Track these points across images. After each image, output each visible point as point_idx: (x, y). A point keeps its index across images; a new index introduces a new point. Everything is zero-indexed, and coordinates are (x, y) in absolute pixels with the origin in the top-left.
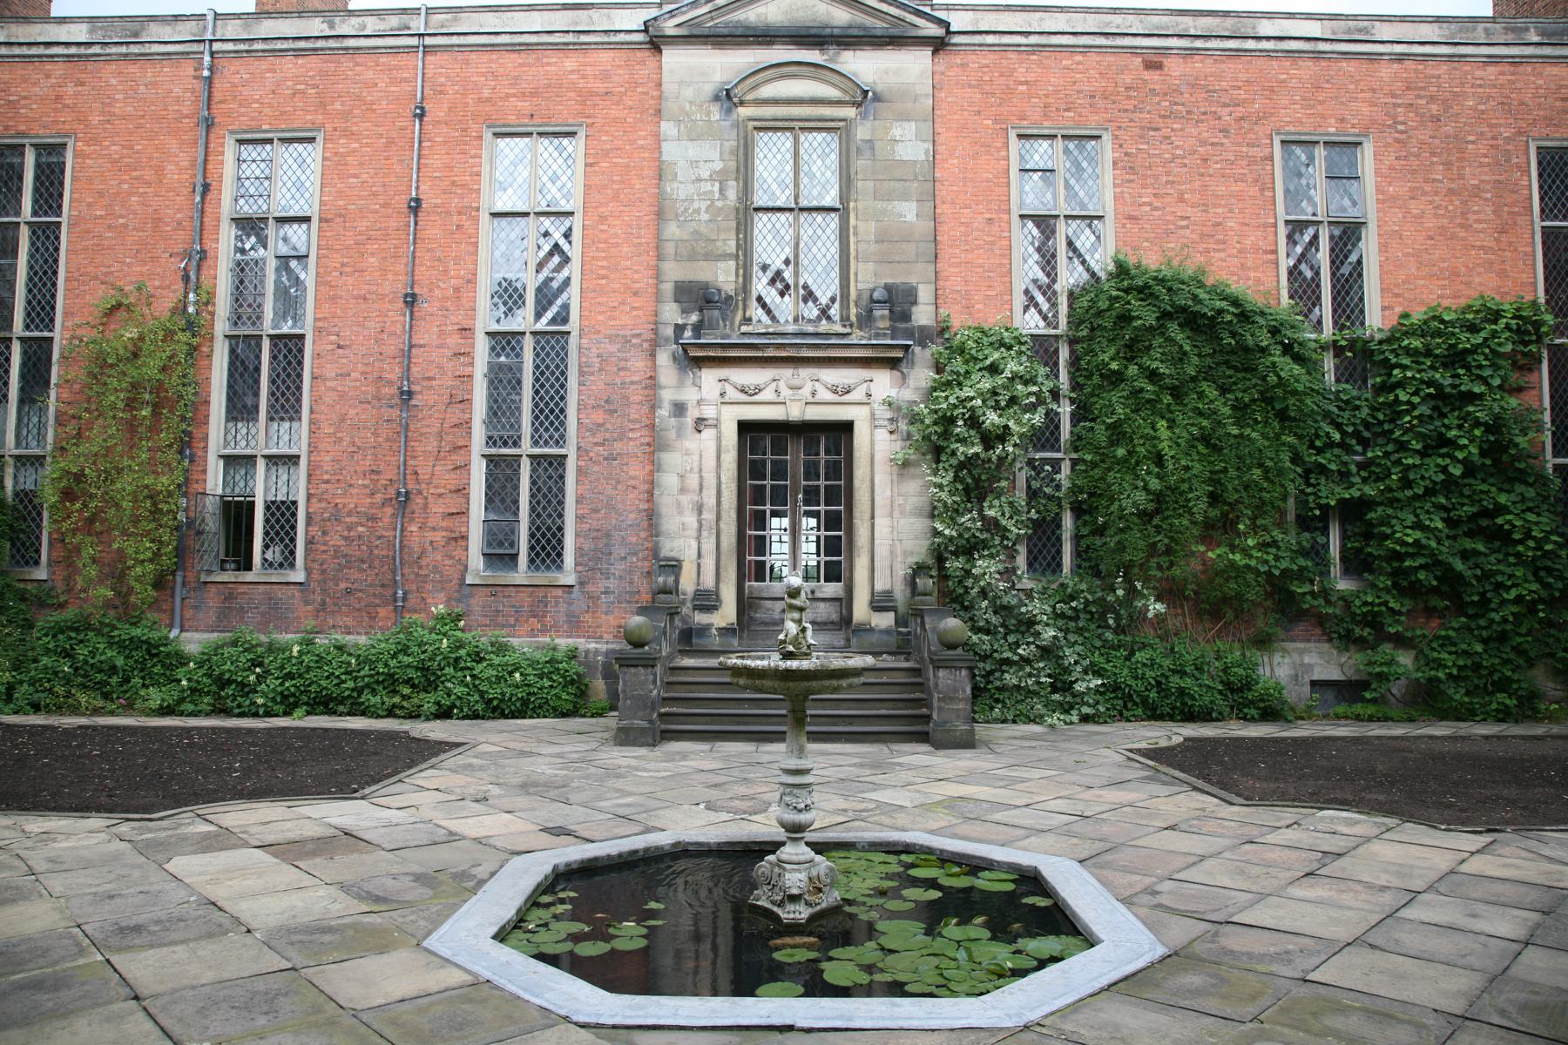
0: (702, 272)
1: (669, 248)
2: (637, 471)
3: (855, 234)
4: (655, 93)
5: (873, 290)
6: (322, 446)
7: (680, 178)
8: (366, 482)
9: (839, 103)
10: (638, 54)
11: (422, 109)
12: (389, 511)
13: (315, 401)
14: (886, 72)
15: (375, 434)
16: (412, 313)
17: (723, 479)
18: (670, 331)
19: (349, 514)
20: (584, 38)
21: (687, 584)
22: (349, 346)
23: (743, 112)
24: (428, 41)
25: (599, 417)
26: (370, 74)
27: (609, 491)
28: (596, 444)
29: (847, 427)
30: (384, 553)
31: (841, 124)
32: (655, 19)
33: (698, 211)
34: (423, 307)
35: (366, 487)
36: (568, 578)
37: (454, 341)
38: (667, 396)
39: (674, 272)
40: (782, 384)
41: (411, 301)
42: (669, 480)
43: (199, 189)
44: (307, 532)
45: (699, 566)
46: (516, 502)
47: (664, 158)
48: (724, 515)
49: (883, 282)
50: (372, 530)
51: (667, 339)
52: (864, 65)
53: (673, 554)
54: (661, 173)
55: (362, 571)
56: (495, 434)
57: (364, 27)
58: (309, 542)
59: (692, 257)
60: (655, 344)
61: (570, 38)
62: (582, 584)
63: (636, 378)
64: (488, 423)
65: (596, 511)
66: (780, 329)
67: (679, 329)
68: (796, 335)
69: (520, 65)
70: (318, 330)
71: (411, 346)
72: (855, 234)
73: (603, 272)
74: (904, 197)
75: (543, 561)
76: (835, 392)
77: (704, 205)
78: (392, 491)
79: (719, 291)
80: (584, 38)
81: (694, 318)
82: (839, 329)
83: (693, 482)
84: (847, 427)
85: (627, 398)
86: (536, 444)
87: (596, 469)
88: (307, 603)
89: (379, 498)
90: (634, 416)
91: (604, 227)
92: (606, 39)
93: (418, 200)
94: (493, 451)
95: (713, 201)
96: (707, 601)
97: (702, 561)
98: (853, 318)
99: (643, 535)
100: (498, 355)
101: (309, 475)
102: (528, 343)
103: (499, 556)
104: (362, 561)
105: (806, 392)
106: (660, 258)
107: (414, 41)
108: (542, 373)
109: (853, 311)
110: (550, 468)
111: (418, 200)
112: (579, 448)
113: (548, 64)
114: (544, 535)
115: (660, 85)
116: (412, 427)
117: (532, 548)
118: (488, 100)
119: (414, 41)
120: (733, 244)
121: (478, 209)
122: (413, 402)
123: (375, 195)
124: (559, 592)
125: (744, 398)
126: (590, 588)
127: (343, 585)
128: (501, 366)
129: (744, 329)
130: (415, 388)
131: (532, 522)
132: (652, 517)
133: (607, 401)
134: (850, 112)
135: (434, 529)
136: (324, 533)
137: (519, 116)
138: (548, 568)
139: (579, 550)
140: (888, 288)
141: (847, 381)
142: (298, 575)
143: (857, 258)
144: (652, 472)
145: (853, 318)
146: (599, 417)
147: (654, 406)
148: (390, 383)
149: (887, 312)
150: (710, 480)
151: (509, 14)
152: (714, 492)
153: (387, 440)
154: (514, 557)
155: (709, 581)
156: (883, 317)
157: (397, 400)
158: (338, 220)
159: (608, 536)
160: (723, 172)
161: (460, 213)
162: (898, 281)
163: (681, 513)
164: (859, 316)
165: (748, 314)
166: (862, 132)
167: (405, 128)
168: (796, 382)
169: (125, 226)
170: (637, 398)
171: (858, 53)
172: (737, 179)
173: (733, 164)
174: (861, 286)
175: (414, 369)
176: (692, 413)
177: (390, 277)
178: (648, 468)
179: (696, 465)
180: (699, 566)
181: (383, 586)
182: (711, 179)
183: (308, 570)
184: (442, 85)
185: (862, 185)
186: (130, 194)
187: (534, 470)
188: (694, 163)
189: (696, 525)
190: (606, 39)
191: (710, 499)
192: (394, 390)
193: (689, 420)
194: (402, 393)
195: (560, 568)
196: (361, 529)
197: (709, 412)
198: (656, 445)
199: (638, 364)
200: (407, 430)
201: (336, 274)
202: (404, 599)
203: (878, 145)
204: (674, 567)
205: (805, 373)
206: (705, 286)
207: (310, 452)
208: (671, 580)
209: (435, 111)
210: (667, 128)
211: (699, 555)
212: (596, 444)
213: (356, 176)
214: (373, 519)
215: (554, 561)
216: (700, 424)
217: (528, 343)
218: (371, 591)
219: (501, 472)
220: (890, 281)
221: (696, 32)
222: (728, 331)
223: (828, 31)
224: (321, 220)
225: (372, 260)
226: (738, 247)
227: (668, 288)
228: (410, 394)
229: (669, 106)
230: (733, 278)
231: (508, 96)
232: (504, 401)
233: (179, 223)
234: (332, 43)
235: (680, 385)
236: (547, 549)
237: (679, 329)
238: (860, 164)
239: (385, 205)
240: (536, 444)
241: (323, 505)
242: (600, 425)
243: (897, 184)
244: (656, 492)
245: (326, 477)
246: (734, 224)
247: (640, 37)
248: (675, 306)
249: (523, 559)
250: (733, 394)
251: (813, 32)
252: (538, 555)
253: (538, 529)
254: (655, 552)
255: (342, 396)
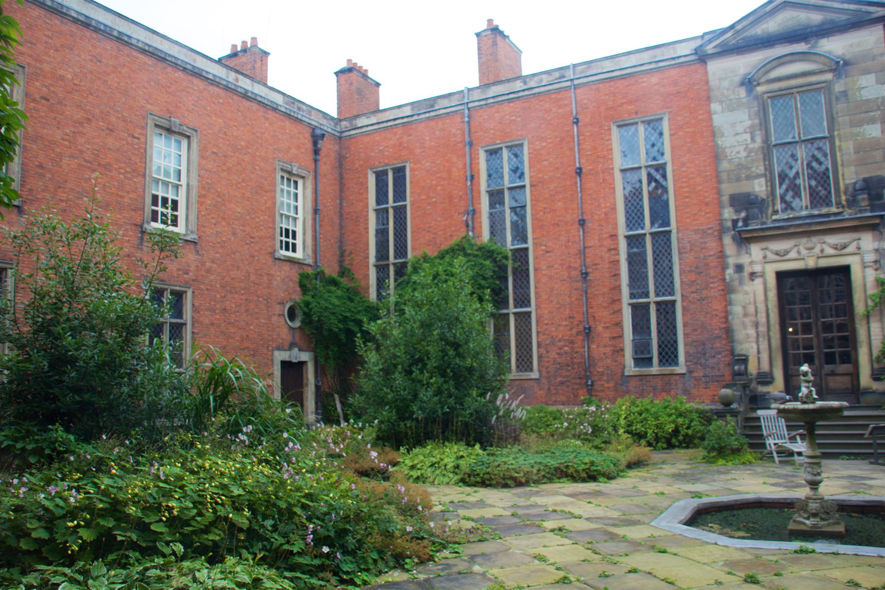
0: (744, 187)
1: (724, 176)
2: (717, 306)
3: (840, 150)
4: (706, 88)
5: (855, 183)
6: (542, 306)
7: (726, 134)
8: (567, 323)
9: (821, 72)
10: (693, 67)
11: (577, 119)
12: (581, 337)
13: (537, 282)
14: (851, 46)
15: (570, 297)
16: (583, 230)
17: (770, 306)
18: (729, 224)
19: (560, 341)
20: (661, 64)
21: (752, 368)
22: (552, 251)
23: (760, 89)
24: (576, 82)
25: (692, 277)
26: (547, 105)
27: (702, 319)
28: (692, 292)
29: (845, 270)
30: (580, 360)
31: (824, 85)
32: (701, 46)
33: (738, 152)
34: (589, 224)
35: (566, 325)
36: (681, 369)
37: (608, 243)
38: (731, 261)
39: (728, 189)
40: (801, 248)
41: (582, 223)
42: (737, 309)
43: (469, 178)
44: (538, 352)
45: (759, 358)
46: (649, 328)
47: (715, 124)
48: (772, 328)
49: (862, 177)
50: (572, 348)
51: (728, 229)
52: (835, 46)
53: (743, 352)
54: (713, 134)
55: (568, 371)
56: (635, 291)
57: (541, 81)
58: (540, 357)
59: (738, 179)
60: (722, 231)
61: (653, 66)
62: (690, 372)
63: (711, 253)
64: (631, 286)
65: (695, 330)
66: (797, 214)
67: (735, 222)
68: (807, 217)
69: (627, 86)
70: (535, 244)
71: (585, 248)
72: (840, 150)
73: (686, 195)
74: (872, 121)
75: (667, 361)
76: (836, 249)
77: (741, 149)
78: (581, 327)
79: (757, 197)
80: (661, 64)
81: (743, 215)
82: (834, 210)
83: (751, 309)
84: (845, 270)
85: (708, 265)
86: (657, 295)
87: (693, 306)
88: (541, 389)
89: (574, 331)
90: (712, 274)
91: (684, 169)
92: (673, 62)
93: (580, 169)
94: (634, 301)
95: (747, 145)
96: (766, 379)
97: (760, 356)
98: (844, 203)
99: (724, 342)
100: (632, 248)
101: (537, 321)
102: (648, 239)
103: (642, 360)
104: (568, 366)
105: (817, 250)
106: (719, 182)
107: (569, 84)
108: (658, 255)
109: (843, 198)
110: (666, 310)
111: (580, 169)
112: (682, 296)
113: (642, 82)
114: (666, 346)
115: (707, 82)
116: (589, 291)
117: (660, 353)
118: (612, 108)
119: (569, 84)
120: (762, 168)
121: (613, 169)
122: (588, 278)
123: (557, 169)
124: (677, 377)
125: (777, 258)
126: (695, 374)
127: (559, 379)
128: (635, 254)
129: (774, 217)
130: (589, 270)
131: (659, 339)
132: (728, 332)
133: (696, 268)
134: (829, 76)
135: (605, 346)
136: (547, 352)
137: (630, 114)
138: (670, 365)
139: (687, 353)
140: (865, 180)
141: (843, 241)
142: (535, 375)
143: (842, 165)
144: (726, 306)
145: (844, 203)
146: (692, 277)
147: (724, 267)
148: (575, 269)
149: (866, 196)
150: (762, 308)
151: (618, 59)
152: (764, 315)
153: (577, 300)
154: (650, 359)
155: (765, 367)
156: (863, 199)
157: (579, 278)
158: (540, 185)
159: (704, 344)
160: (752, 127)
161: (603, 172)
162: (873, 174)
163: (745, 327)
164: (847, 201)
165: (776, 208)
166: (838, 87)
167: (568, 131)
168: (809, 245)
169: (435, 202)
170: (715, 264)
171: (831, 38)
172: (760, 130)
173: (757, 121)
174: (847, 182)
175: (588, 260)
176: (748, 270)
177: (570, 211)
178: (724, 304)
179: (752, 300)
180: (759, 358)
181: (580, 378)
182: (745, 132)
183: (540, 371)
184: (586, 104)
185: (843, 119)
186: (437, 185)
187: (658, 310)
188: (733, 125)
189: (755, 335)
190: (673, 62)
191: (762, 319)
192: (578, 272)
193: (746, 274)
194: (582, 274)
195: (677, 364)
196: (566, 348)
197: (757, 268)
198: (728, 290)
199: (712, 244)
200: (586, 293)
201: (542, 213)
202: (592, 385)
203: (850, 93)
204: (744, 360)
205: (815, 239)
206: (748, 195)
207: (537, 309)
208: (743, 367)
209: (584, 119)
210: (715, 107)
211: (759, 352)
212: (692, 292)
213: (546, 160)
214: (572, 342)
215: (673, 360)
216: (753, 275)
217: (648, 239)
218: (574, 381)
219: (640, 312)
220: (866, 176)
221: (725, 48)
222: (764, 220)
223: (809, 30)
224: (531, 186)
225: (559, 204)
226: (766, 169)
227: (725, 199)
228: (586, 274)
229: (715, 93)
230: (764, 188)
231: (622, 104)
232: (638, 272)
233: (461, 197)
234: (526, 93)
235: (739, 254)
236: (668, 355)
237: (735, 222)
238: (839, 107)
239: (563, 174)
240: (657, 295)
241: (546, 337)
242: (693, 282)
243: (866, 115)
244: (730, 318)
245: (546, 322)
246: (761, 156)
247: (693, 58)
248: (731, 209)
249: (655, 360)
250: (771, 257)
251: (799, 32)
252: (664, 357)
253: (663, 342)
254: (732, 352)
255: (551, 277)
